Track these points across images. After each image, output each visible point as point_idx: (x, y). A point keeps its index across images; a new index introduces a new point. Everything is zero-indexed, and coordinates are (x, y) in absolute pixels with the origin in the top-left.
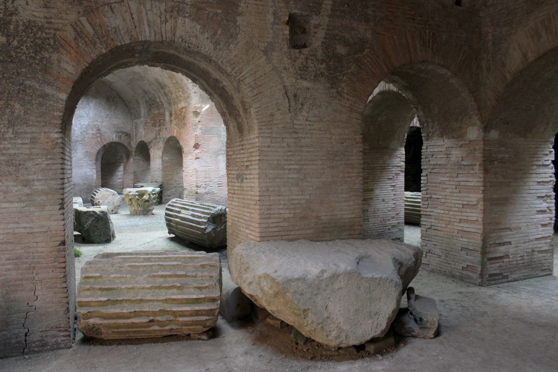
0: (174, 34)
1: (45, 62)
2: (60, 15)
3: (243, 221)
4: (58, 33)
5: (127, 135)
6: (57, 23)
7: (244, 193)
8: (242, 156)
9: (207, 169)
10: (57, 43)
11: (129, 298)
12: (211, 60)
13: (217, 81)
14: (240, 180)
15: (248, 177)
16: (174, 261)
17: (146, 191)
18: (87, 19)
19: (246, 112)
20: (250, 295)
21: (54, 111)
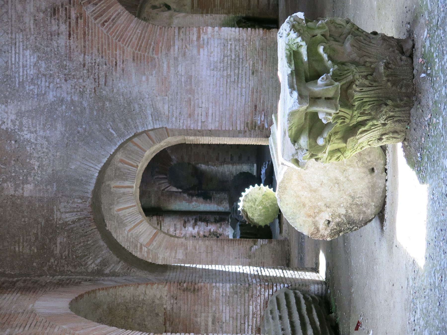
17: (292, 114)
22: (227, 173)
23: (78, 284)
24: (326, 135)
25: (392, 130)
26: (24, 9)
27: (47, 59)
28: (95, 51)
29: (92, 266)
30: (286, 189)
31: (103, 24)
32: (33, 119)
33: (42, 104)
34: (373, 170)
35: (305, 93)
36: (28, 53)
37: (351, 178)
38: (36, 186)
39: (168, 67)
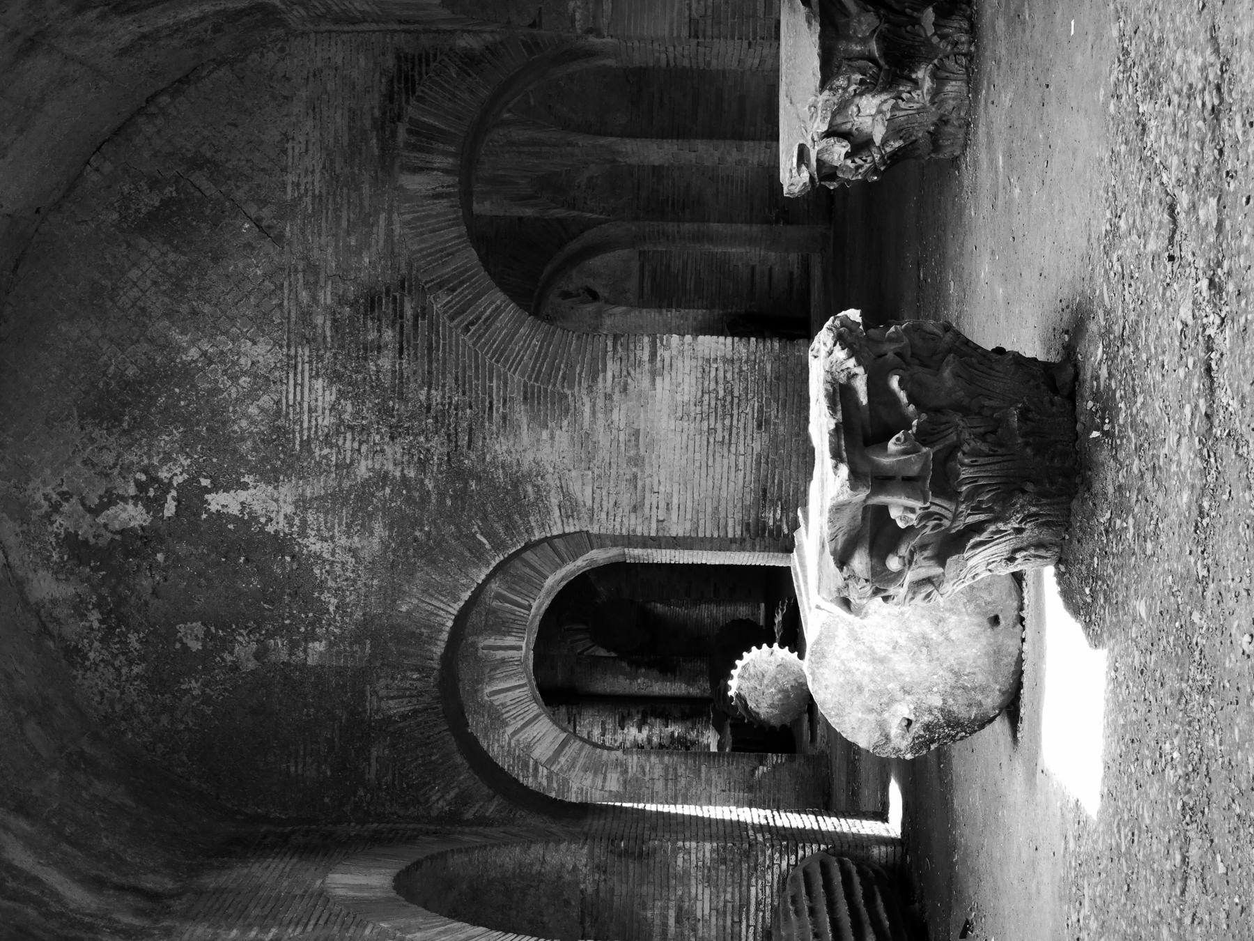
17: (838, 509)
22: (707, 621)
23: (411, 839)
24: (904, 551)
25: (1034, 541)
26: (314, 299)
27: (356, 397)
28: (450, 381)
29: (440, 802)
30: (824, 656)
31: (467, 329)
32: (326, 513)
33: (346, 484)
34: (995, 621)
35: (865, 468)
36: (319, 384)
37: (953, 635)
38: (331, 645)
39: (594, 413)
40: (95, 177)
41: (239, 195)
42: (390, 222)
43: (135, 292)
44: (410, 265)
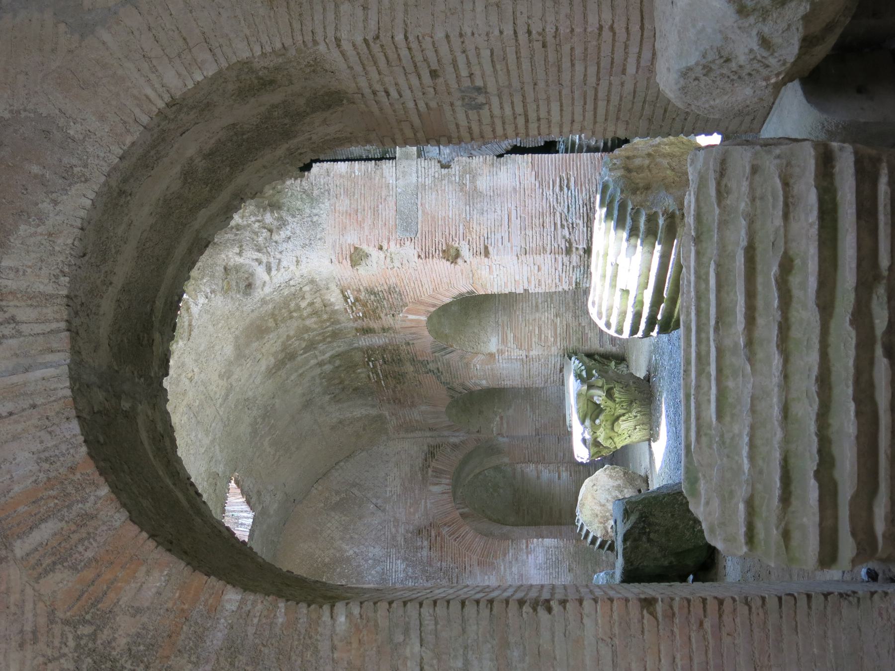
0: (48, 297)
1: (142, 648)
2: (13, 609)
3: (604, 84)
4: (60, 614)
5: (433, 455)
6: (35, 615)
7: (516, 84)
8: (407, 94)
9: (516, 223)
10: (88, 617)
11: (814, 417)
12: (122, 193)
13: (188, 175)
14: (481, 99)
15: (464, 73)
16: (707, 282)
17: (579, 395)
18: (19, 537)
19: (272, 82)
20: (808, 42)
21: (272, 625)
26: (397, 531)
28: (449, 559)
31: (455, 540)
36: (399, 562)
39: (505, 568)
40: (315, 491)
41: (369, 495)
42: (426, 502)
43: (329, 531)
44: (433, 518)
